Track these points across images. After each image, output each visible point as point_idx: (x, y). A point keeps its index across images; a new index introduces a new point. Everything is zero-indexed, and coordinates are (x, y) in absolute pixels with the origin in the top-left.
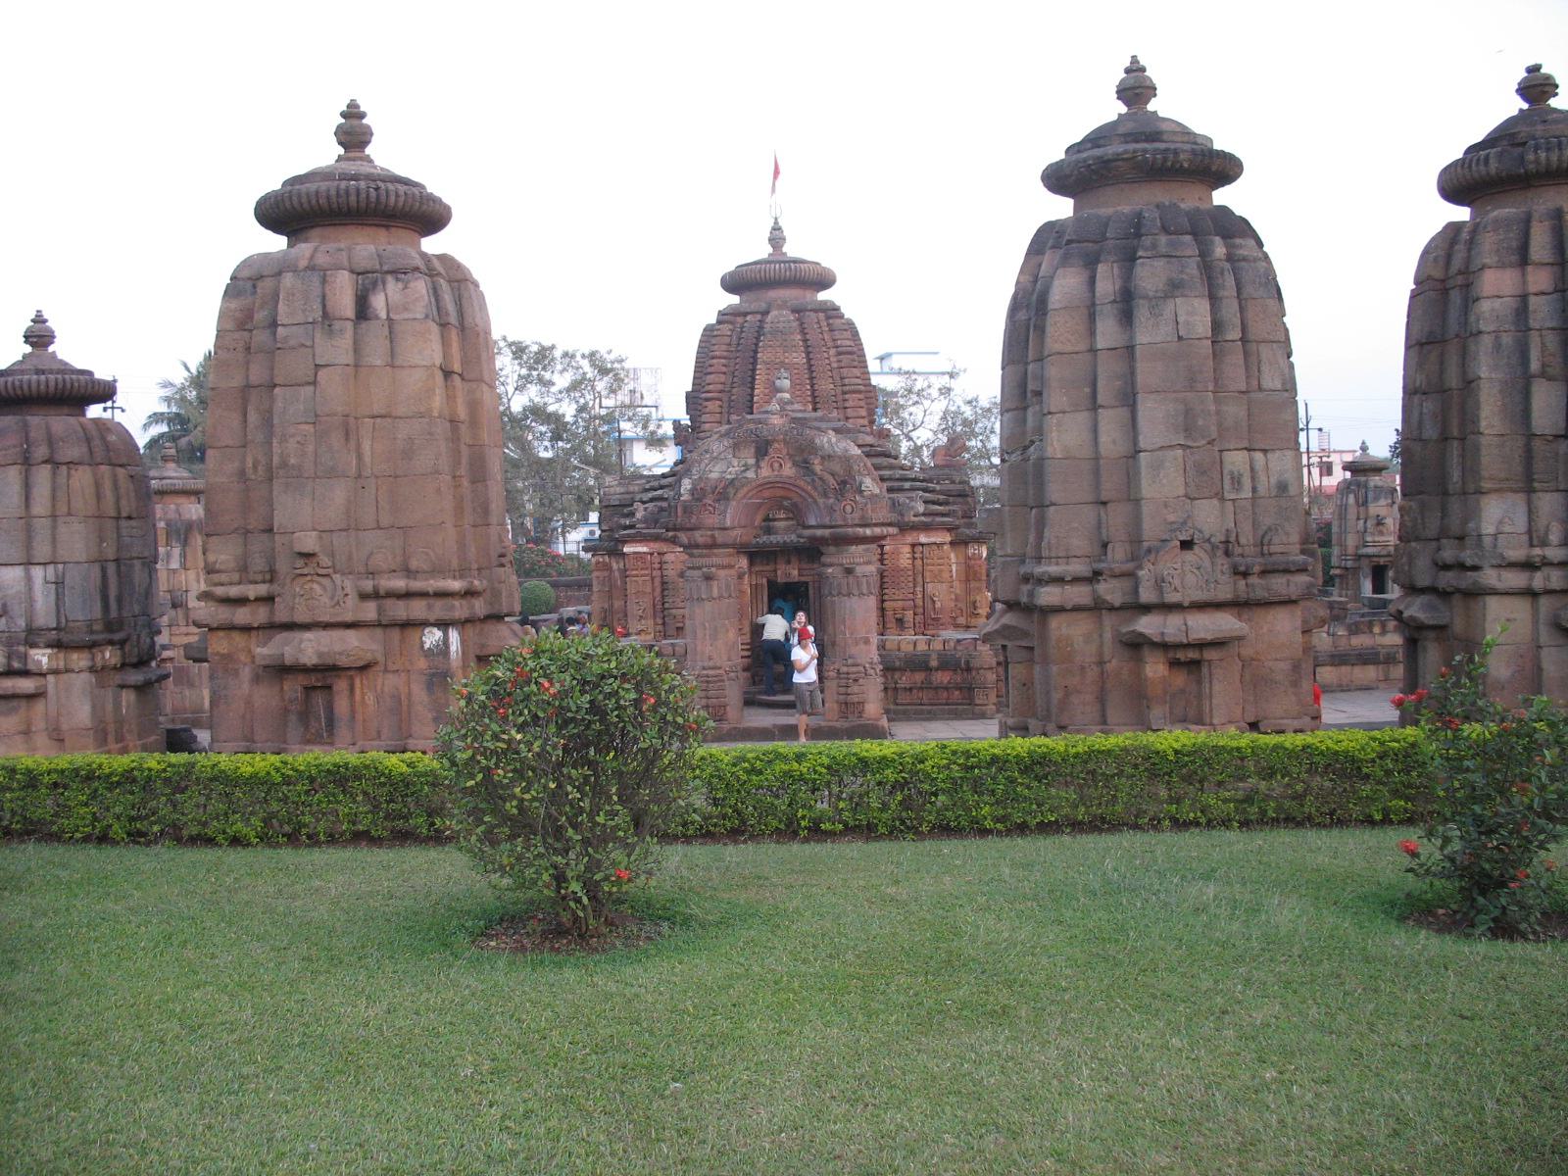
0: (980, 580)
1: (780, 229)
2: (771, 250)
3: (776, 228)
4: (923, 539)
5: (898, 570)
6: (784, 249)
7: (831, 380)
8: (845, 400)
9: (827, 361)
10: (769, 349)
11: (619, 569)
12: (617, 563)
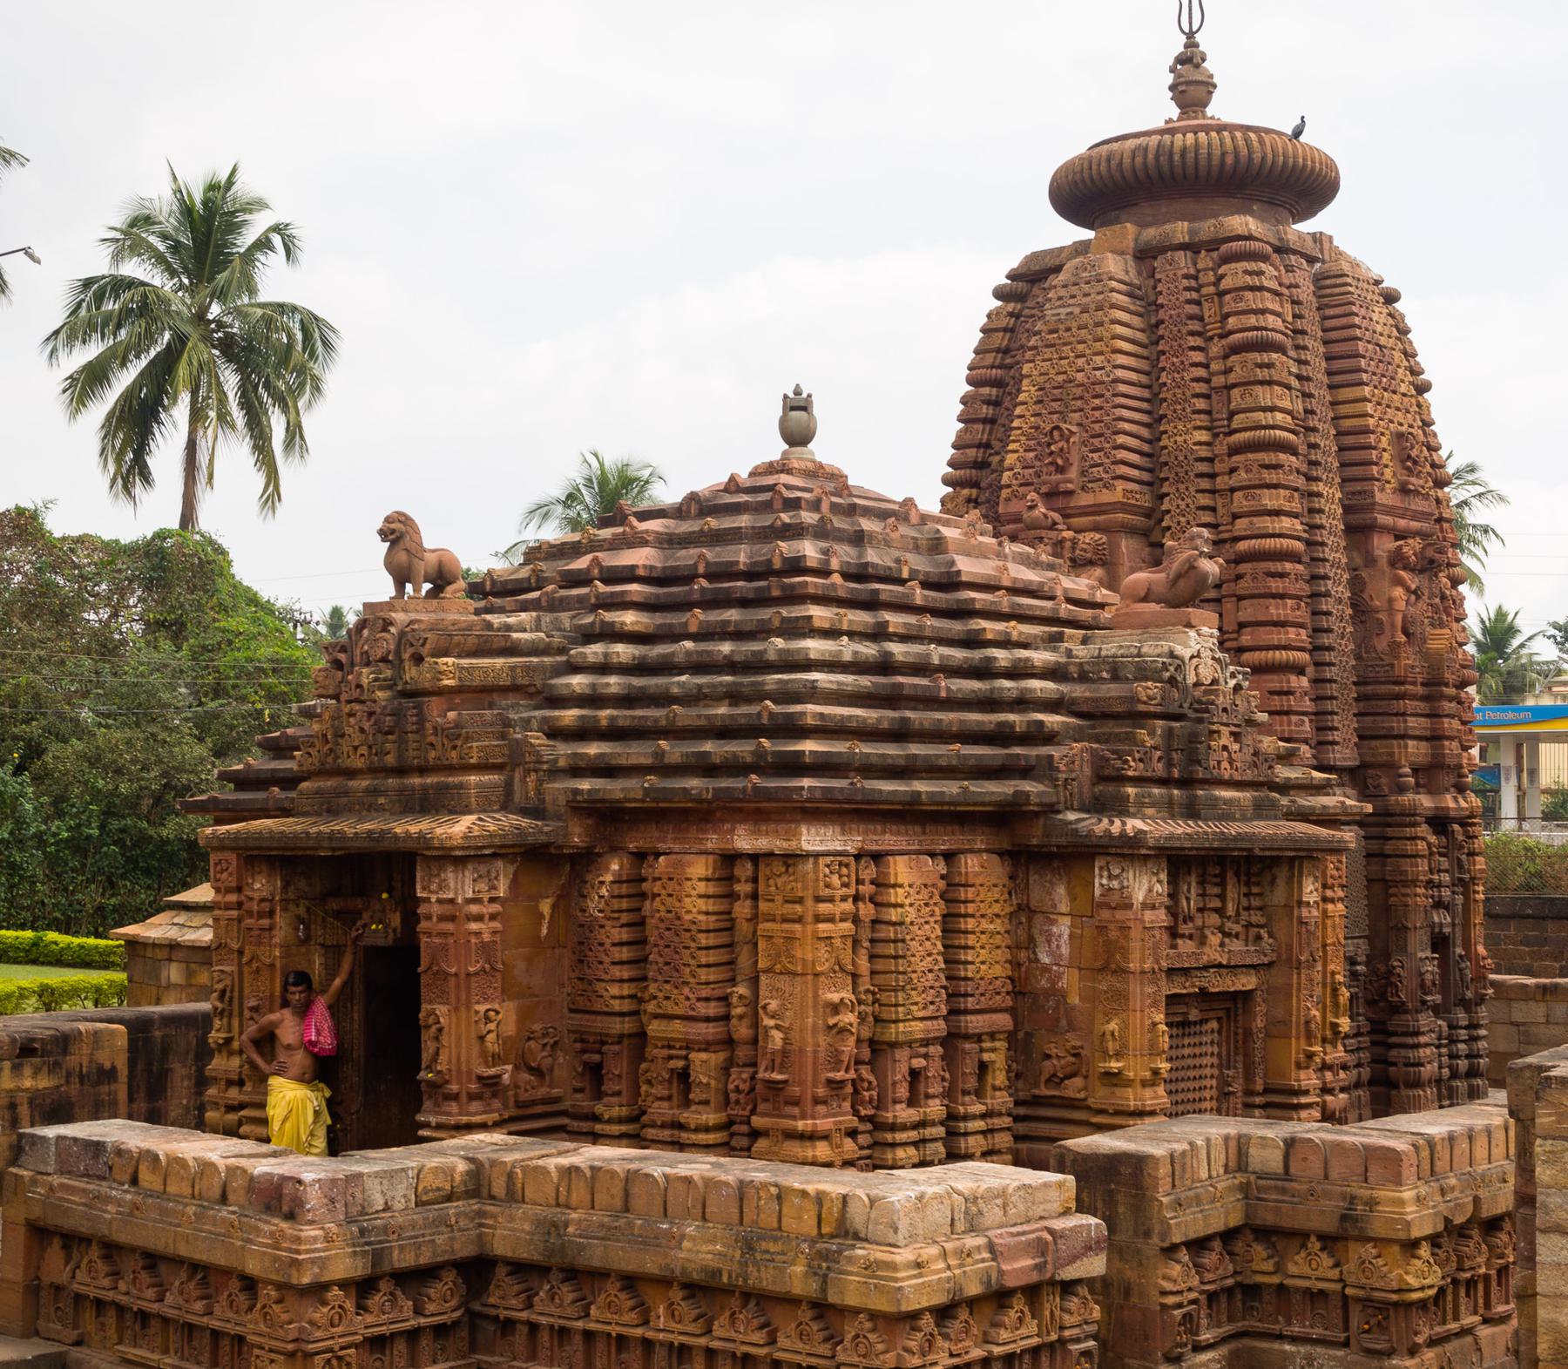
0: (1122, 972)
2: (1174, 112)
3: (1190, 59)
4: (744, 841)
5: (675, 923)
6: (1210, 111)
7: (1201, 420)
8: (1233, 470)
9: (1201, 372)
10: (1048, 353)
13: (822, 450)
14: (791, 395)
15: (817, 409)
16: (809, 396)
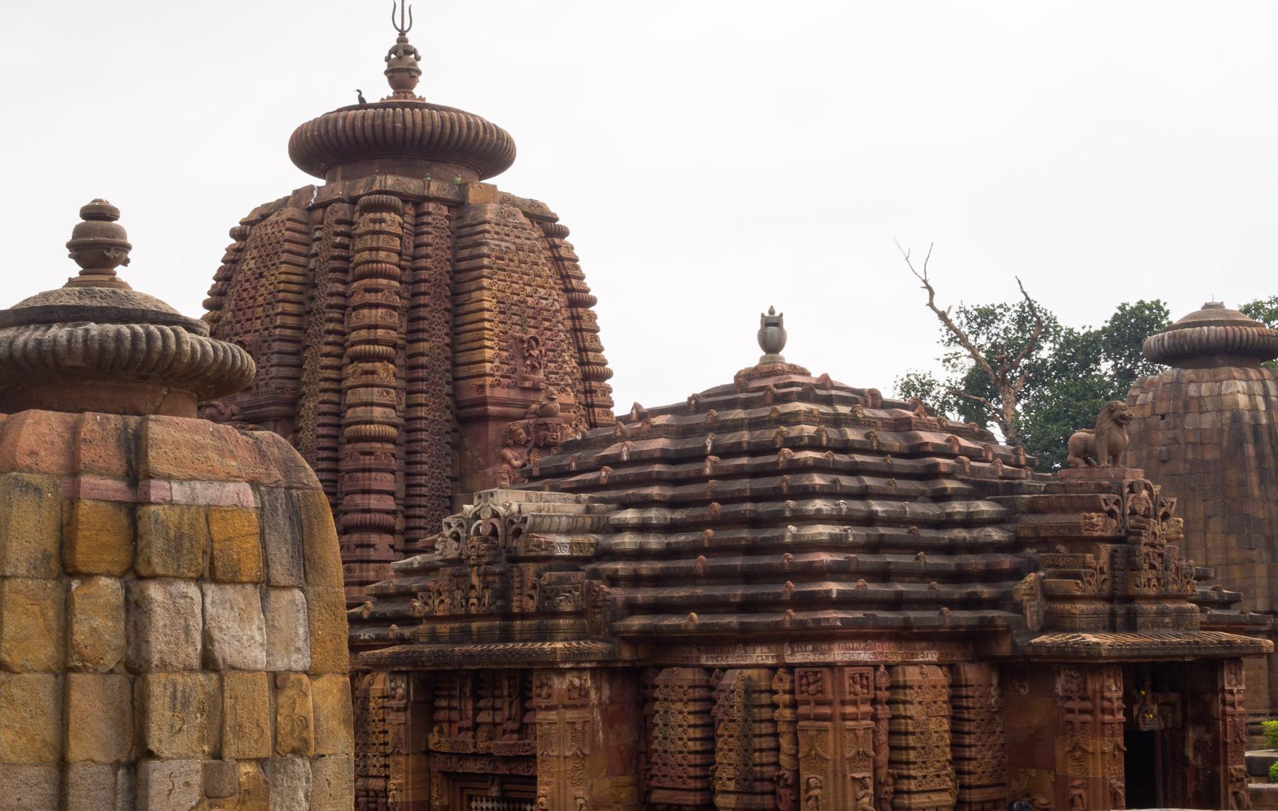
1: (409, 51)
10: (502, 275)
11: (600, 703)
12: (599, 689)
13: (789, 355)
14: (767, 314)
15: (786, 326)
16: (781, 315)
